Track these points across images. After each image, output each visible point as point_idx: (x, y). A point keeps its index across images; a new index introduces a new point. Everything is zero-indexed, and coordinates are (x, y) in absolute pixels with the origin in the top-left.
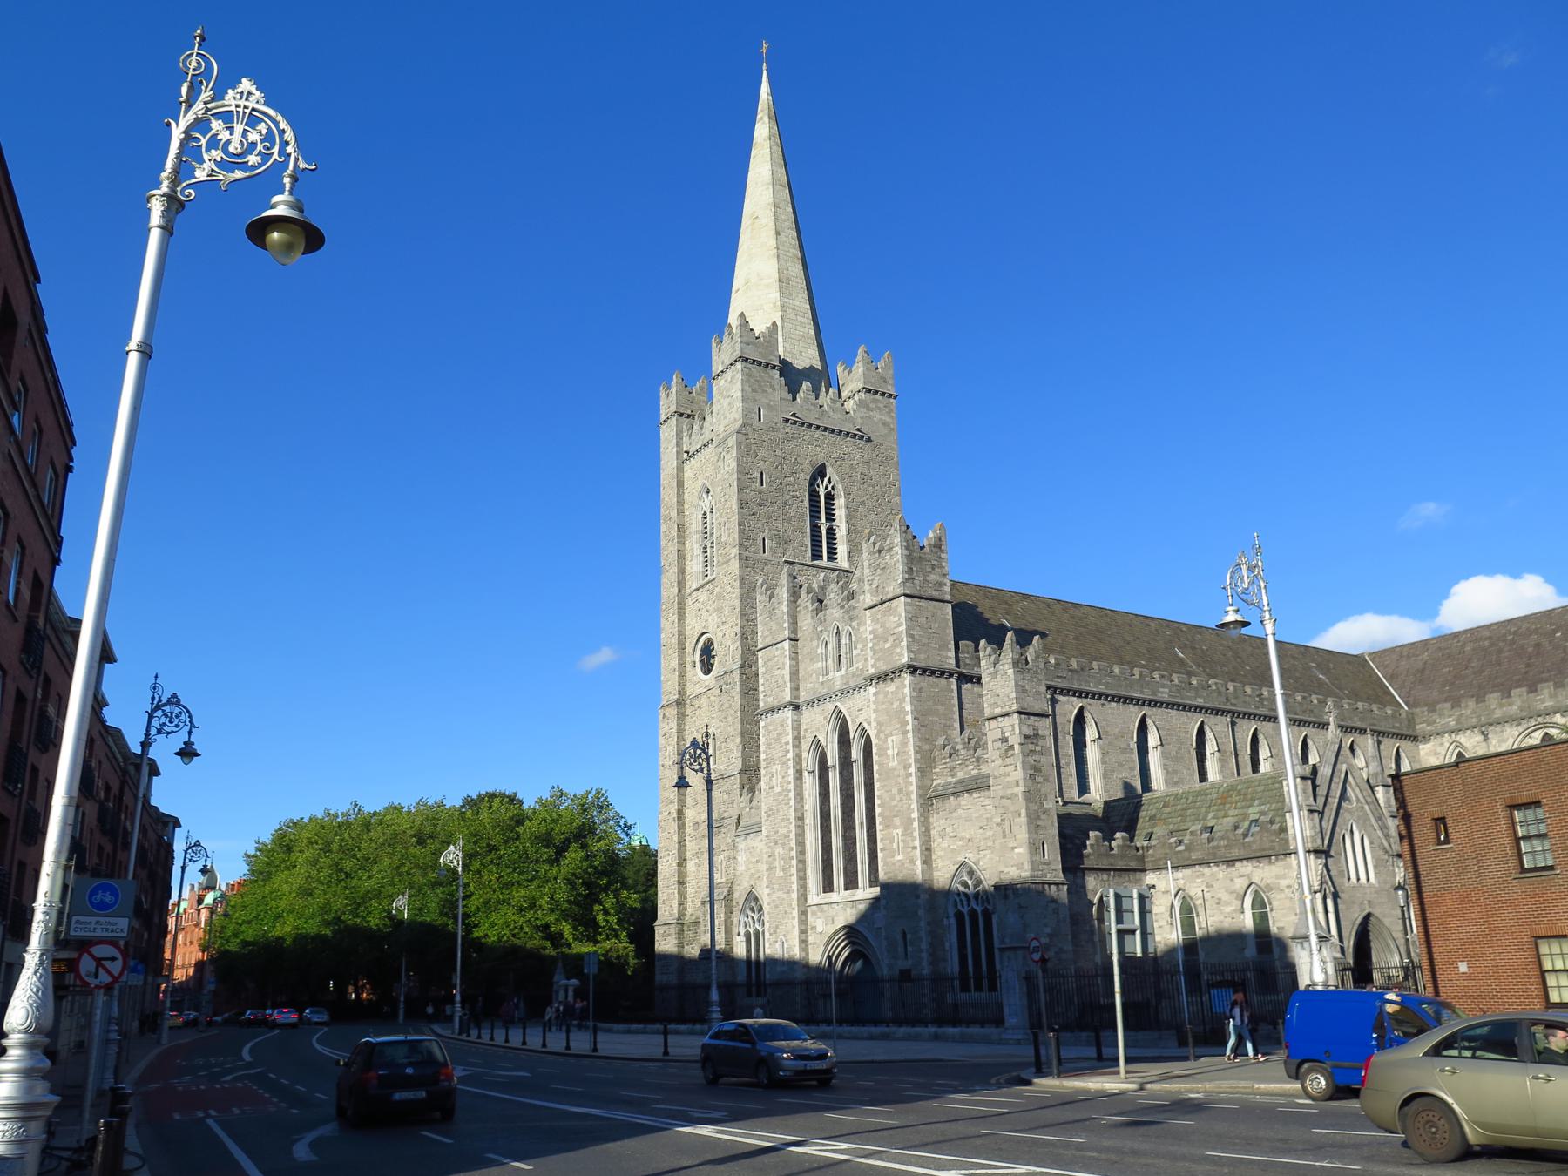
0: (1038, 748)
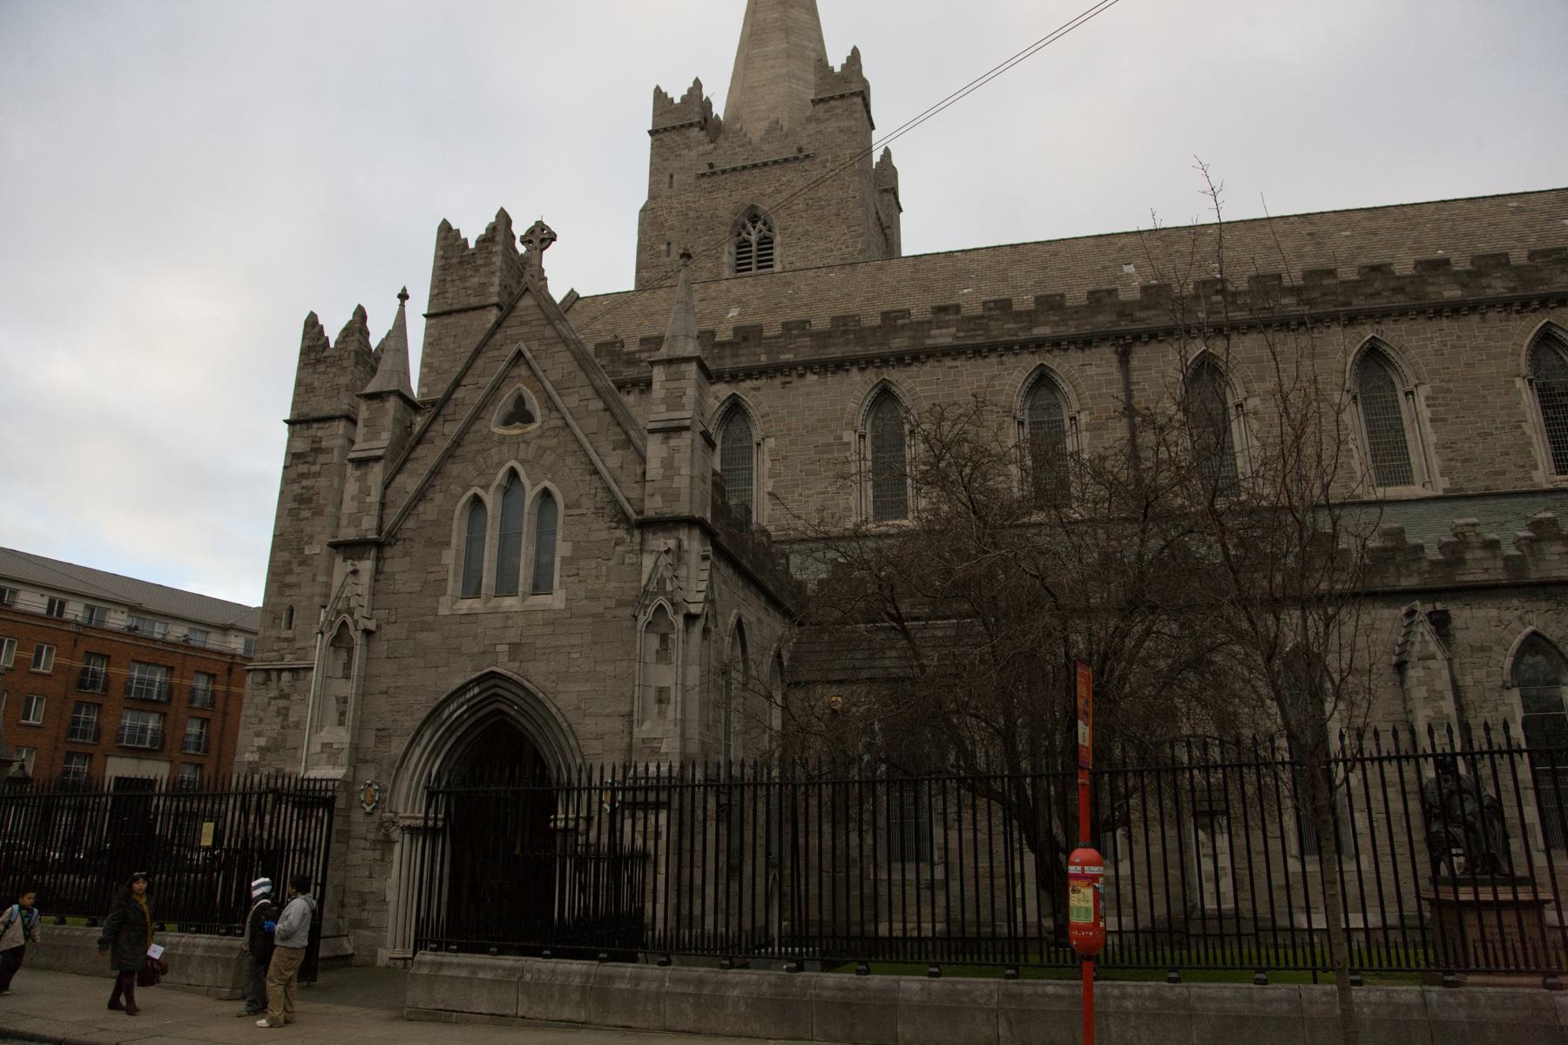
0: (316, 468)
